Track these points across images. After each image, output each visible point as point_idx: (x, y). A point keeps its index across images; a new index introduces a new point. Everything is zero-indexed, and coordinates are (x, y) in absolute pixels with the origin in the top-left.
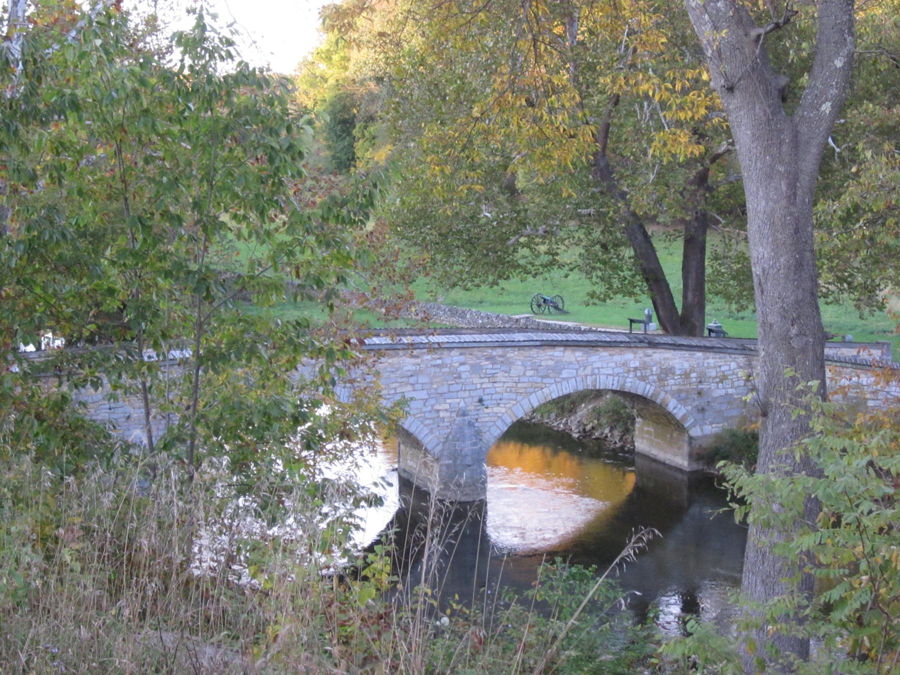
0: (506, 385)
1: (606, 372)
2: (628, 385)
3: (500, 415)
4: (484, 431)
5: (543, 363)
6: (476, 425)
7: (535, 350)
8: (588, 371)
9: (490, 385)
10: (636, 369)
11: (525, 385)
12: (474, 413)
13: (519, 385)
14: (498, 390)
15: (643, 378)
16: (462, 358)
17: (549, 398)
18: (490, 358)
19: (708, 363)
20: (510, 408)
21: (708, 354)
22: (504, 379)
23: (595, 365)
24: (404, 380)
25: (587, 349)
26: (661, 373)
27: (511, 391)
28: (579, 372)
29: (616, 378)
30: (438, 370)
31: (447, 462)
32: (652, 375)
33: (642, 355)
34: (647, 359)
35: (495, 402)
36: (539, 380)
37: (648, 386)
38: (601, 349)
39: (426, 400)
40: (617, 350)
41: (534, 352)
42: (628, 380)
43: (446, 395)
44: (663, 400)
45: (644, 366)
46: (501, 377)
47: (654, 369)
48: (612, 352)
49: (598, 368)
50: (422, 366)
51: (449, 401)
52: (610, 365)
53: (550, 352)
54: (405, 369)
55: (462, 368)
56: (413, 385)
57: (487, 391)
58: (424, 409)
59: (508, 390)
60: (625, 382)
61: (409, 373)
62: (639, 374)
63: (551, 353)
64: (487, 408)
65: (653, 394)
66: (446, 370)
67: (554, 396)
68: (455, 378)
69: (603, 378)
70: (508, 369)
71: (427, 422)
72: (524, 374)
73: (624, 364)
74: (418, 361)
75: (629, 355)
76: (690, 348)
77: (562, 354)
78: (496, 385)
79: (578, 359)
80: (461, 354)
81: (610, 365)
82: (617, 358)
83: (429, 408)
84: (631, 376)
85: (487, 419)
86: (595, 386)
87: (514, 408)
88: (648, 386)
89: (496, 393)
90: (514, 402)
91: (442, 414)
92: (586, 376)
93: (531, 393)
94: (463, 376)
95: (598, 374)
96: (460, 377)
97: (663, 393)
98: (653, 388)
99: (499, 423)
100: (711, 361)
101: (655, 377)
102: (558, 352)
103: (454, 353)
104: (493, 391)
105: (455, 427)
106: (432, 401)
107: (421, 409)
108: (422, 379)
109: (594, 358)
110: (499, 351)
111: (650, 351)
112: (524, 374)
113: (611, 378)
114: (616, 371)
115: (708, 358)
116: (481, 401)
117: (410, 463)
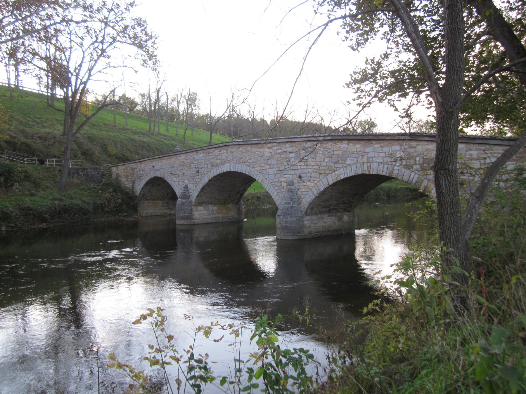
0: (314, 167)
1: (377, 160)
2: (396, 172)
3: (310, 187)
4: (302, 197)
5: (335, 153)
6: (299, 193)
7: (330, 143)
8: (365, 159)
9: (305, 167)
10: (401, 159)
11: (325, 168)
12: (297, 185)
13: (321, 168)
14: (310, 170)
15: (408, 167)
16: (290, 149)
17: (339, 179)
18: (304, 149)
19: (471, 155)
20: (316, 184)
21: (472, 146)
22: (312, 164)
23: (370, 155)
24: (266, 161)
25: (364, 142)
26: (424, 163)
27: (316, 172)
28: (359, 160)
29: (386, 166)
30: (279, 156)
32: (415, 164)
33: (407, 147)
34: (412, 150)
35: (308, 179)
36: (333, 165)
37: (413, 174)
38: (374, 142)
39: (275, 174)
40: (386, 143)
41: (329, 145)
42: (396, 168)
43: (285, 172)
44: (426, 188)
46: (310, 161)
47: (418, 159)
48: (382, 145)
49: (372, 157)
51: (285, 176)
52: (381, 155)
53: (339, 145)
54: (266, 155)
55: (292, 155)
58: (275, 180)
59: (315, 171)
60: (393, 170)
61: (268, 158)
62: (404, 163)
64: (304, 182)
65: (417, 182)
66: (283, 156)
67: (342, 177)
68: (287, 161)
69: (376, 165)
70: (314, 157)
71: (276, 188)
72: (324, 160)
73: (391, 154)
74: (271, 150)
75: (396, 147)
76: (474, 143)
77: (347, 146)
78: (308, 167)
79: (358, 150)
80: (291, 146)
81: (381, 155)
82: (386, 149)
83: (277, 180)
84: (398, 164)
85: (303, 190)
86: (370, 171)
87: (318, 184)
88: (413, 174)
89: (309, 172)
90: (318, 180)
92: (364, 163)
93: (328, 174)
94: (292, 160)
95: (372, 162)
96: (289, 161)
97: (425, 183)
98: (417, 176)
99: (310, 193)
100: (475, 153)
101: (418, 167)
102: (344, 145)
103: (288, 145)
104: (306, 171)
106: (278, 176)
107: (273, 180)
108: (274, 162)
111: (413, 143)
112: (324, 160)
113: (381, 165)
114: (386, 159)
115: (471, 150)
116: (300, 177)
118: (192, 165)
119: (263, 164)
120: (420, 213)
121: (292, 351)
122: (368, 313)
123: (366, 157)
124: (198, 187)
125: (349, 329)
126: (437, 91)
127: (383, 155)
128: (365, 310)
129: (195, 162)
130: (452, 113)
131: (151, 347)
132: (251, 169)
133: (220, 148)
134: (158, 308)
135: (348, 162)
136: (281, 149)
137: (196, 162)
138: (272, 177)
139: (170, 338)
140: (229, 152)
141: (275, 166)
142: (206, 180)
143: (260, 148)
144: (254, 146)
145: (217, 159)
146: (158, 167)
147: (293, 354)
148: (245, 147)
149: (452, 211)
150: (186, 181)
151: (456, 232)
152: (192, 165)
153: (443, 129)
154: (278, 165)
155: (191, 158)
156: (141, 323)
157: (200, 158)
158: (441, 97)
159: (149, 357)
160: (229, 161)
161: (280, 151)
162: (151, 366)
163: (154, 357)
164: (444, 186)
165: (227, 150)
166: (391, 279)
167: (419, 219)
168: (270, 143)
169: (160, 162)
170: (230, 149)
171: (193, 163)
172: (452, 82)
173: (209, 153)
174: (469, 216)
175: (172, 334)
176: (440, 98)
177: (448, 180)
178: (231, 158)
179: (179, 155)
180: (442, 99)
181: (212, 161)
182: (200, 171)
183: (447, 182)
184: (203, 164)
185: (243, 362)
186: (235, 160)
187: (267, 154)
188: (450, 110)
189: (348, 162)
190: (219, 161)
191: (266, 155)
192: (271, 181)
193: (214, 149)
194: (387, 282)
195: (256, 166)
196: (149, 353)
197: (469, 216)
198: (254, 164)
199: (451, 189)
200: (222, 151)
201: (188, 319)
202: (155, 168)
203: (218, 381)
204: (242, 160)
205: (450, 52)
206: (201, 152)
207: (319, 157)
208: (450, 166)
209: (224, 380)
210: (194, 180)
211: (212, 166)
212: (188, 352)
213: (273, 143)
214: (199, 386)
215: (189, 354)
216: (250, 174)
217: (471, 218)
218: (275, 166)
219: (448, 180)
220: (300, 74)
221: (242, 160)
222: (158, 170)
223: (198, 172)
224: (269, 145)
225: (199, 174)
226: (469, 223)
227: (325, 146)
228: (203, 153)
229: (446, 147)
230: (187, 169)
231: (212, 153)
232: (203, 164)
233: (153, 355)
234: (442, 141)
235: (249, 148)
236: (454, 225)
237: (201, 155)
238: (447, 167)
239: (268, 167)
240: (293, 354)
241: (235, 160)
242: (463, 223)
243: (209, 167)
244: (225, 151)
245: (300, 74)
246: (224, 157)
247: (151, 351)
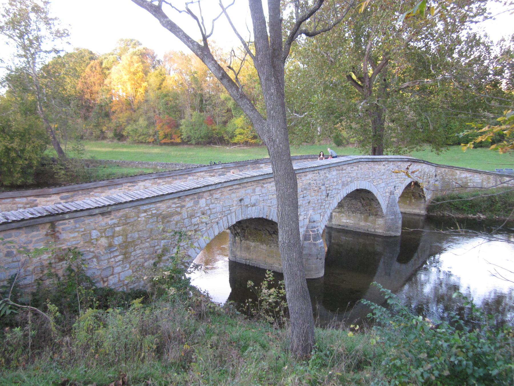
31: (391, 217)
57: (397, 182)
103: (392, 163)
105: (390, 200)
108: (385, 177)
110: (399, 163)
117: (345, 221)
118: (323, 188)
124: (326, 215)
129: (326, 183)
137: (328, 182)
144: (375, 163)
146: (253, 199)
148: (370, 163)
150: (311, 212)
152: (323, 188)
155: (322, 177)
160: (358, 178)
169: (258, 189)
170: (360, 166)
171: (324, 185)
173: (342, 170)
179: (303, 174)
181: (344, 179)
182: (330, 195)
184: (335, 184)
187: (383, 171)
190: (349, 180)
200: (354, 167)
202: (247, 201)
204: (366, 176)
210: (323, 207)
211: (343, 185)
221: (366, 176)
222: (254, 205)
223: (328, 195)
224: (384, 163)
225: (329, 197)
228: (337, 170)
230: (313, 194)
232: (335, 184)
235: (372, 164)
237: (334, 173)
239: (381, 182)
241: (362, 177)
243: (340, 188)
244: (357, 168)
246: (354, 174)
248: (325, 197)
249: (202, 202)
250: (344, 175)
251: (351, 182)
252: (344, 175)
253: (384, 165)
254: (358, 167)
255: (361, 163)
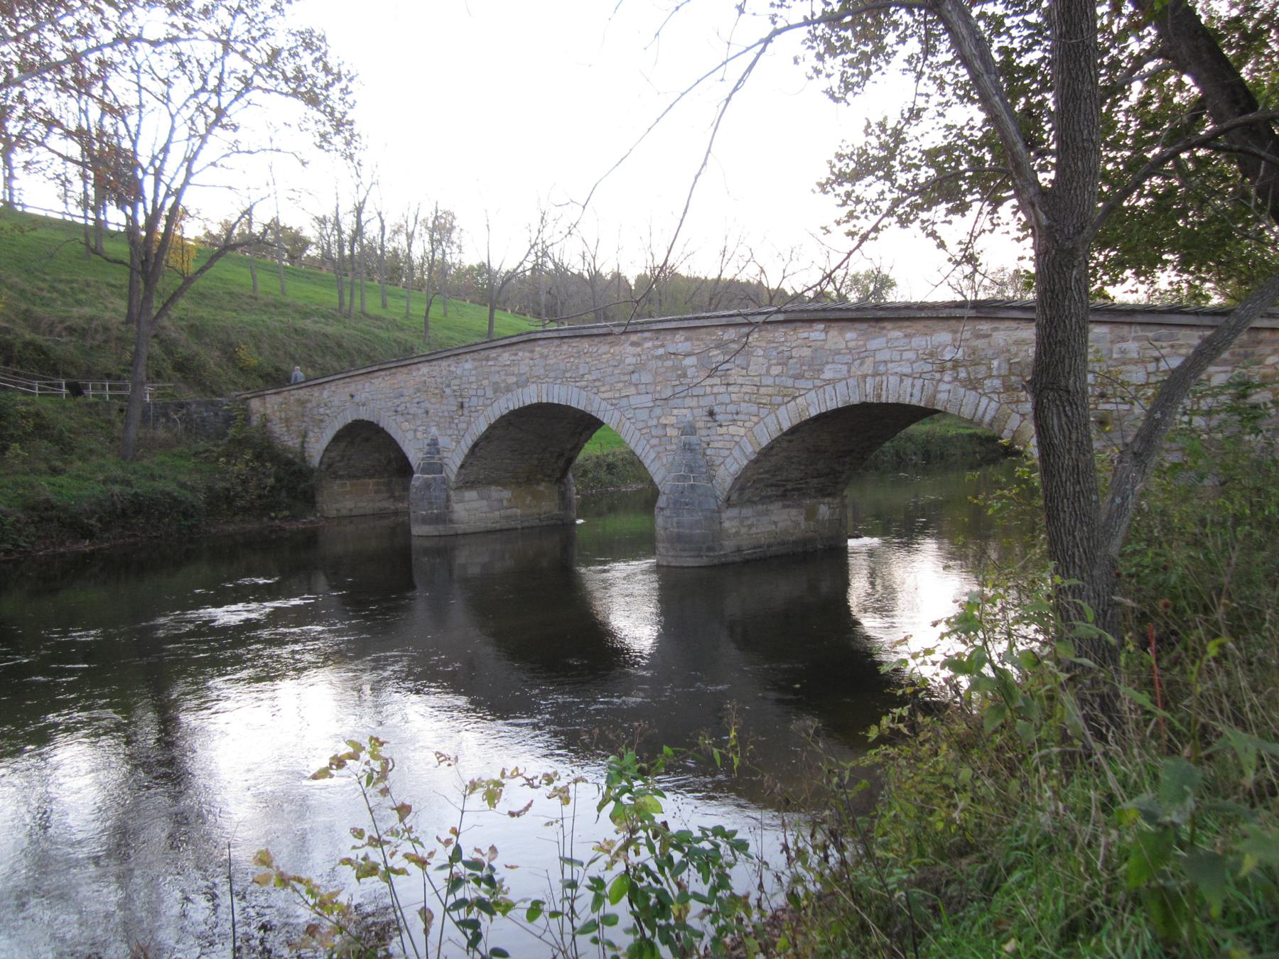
0: (745, 389)
1: (899, 370)
2: (943, 396)
3: (737, 439)
4: (717, 463)
6: (708, 452)
8: (868, 368)
9: (723, 389)
10: (956, 364)
11: (770, 391)
12: (704, 432)
13: (763, 390)
15: (973, 384)
17: (806, 417)
18: (720, 345)
19: (1123, 352)
20: (751, 429)
21: (1125, 330)
22: (740, 380)
23: (880, 357)
24: (627, 378)
25: (865, 326)
26: (1011, 373)
27: (750, 401)
28: (853, 369)
29: (919, 383)
30: (660, 363)
32: (990, 376)
33: (967, 335)
34: (980, 343)
35: (730, 417)
36: (790, 382)
37: (984, 401)
38: (888, 325)
40: (919, 326)
41: (780, 334)
42: (943, 387)
43: (671, 403)
44: (1016, 434)
45: (975, 360)
46: (736, 375)
47: (995, 363)
48: (909, 331)
49: (885, 362)
50: (644, 357)
51: (675, 412)
53: (804, 333)
54: (627, 361)
56: (636, 385)
58: (651, 423)
59: (747, 398)
60: (936, 392)
61: (631, 368)
62: (963, 375)
63: (805, 335)
64: (721, 426)
65: (994, 419)
67: (814, 412)
68: (679, 376)
69: (893, 380)
70: (744, 364)
71: (654, 441)
73: (932, 355)
74: (639, 350)
75: (943, 337)
76: (1130, 324)
77: (823, 336)
78: (730, 389)
79: (851, 344)
80: (687, 339)
82: (918, 342)
83: (654, 422)
84: (947, 378)
85: (720, 445)
86: (880, 396)
88: (984, 401)
89: (732, 402)
90: (755, 419)
91: (670, 431)
93: (779, 405)
94: (690, 372)
95: (885, 373)
96: (685, 375)
97: (1014, 422)
98: (993, 405)
99: (736, 452)
100: (1132, 347)
101: (997, 383)
102: (816, 333)
103: (680, 336)
104: (726, 399)
106: (658, 411)
108: (646, 378)
109: (874, 344)
111: (985, 327)
113: (908, 381)
114: (920, 367)
115: (1123, 339)
118: (448, 391)
119: (621, 385)
120: (1003, 496)
121: (697, 834)
122: (882, 740)
123: (869, 362)
124: (463, 443)
125: (835, 780)
126: (1035, 200)
127: (911, 355)
128: (873, 733)
130: (1072, 253)
131: (359, 833)
132: (592, 396)
133: (514, 348)
134: (372, 738)
135: (828, 375)
136: (662, 346)
137: (457, 382)
138: (643, 414)
139: (404, 810)
140: (536, 355)
141: (651, 388)
142: (481, 426)
143: (612, 344)
144: (597, 340)
145: (507, 375)
147: (699, 840)
148: (575, 342)
149: (1078, 488)
150: (434, 430)
151: (1088, 539)
153: (1053, 292)
154: (656, 384)
156: (332, 776)
157: (466, 373)
158: (1046, 213)
159: (353, 857)
161: (661, 351)
162: (358, 879)
163: (365, 858)
164: (1056, 428)
165: (532, 352)
166: (934, 657)
167: (1000, 510)
168: (636, 332)
170: (538, 349)
171: (449, 386)
172: (1072, 177)
173: (487, 359)
174: (1118, 500)
175: (407, 803)
176: (1043, 217)
177: (1066, 415)
178: (542, 371)
179: (414, 367)
180: (1048, 218)
181: (496, 378)
182: (466, 405)
183: (1064, 419)
184: (474, 386)
185: (582, 864)
186: (552, 374)
188: (1069, 244)
189: (828, 375)
190: (514, 379)
191: (627, 361)
192: (640, 425)
193: (499, 350)
194: (924, 663)
195: (602, 389)
196: (354, 847)
197: (1118, 500)
198: (597, 384)
199: (1074, 437)
200: (520, 354)
201: (444, 764)
202: (357, 399)
203: (520, 913)
204: (568, 375)
205: (1067, 105)
206: (468, 356)
207: (757, 363)
208: (1071, 381)
209: (535, 909)
210: (454, 426)
211: (495, 392)
212: (448, 842)
213: (642, 331)
214: (475, 924)
215: (451, 847)
216: (588, 410)
217: (1122, 504)
218: (651, 388)
219: (1066, 415)
220: (705, 164)
221: (568, 375)
223: (462, 406)
224: (634, 338)
225: (466, 412)
226: (1119, 517)
227: (770, 336)
228: (474, 360)
229: (1060, 333)
230: (433, 400)
231: (495, 359)
232: (474, 386)
233: (361, 853)
234: (1050, 321)
235: (585, 345)
236: (1081, 522)
237: (468, 366)
238: (1063, 383)
239: (632, 390)
240: (699, 840)
241: (552, 374)
242: (1103, 519)
243: (490, 393)
244: (527, 354)
245: (705, 164)
246: (524, 369)
247: (359, 843)
248: (455, 408)
249: (326, 394)
250: (493, 369)
251: (518, 385)
252: (493, 369)
253: (634, 344)
254: (532, 352)
255: (541, 342)
